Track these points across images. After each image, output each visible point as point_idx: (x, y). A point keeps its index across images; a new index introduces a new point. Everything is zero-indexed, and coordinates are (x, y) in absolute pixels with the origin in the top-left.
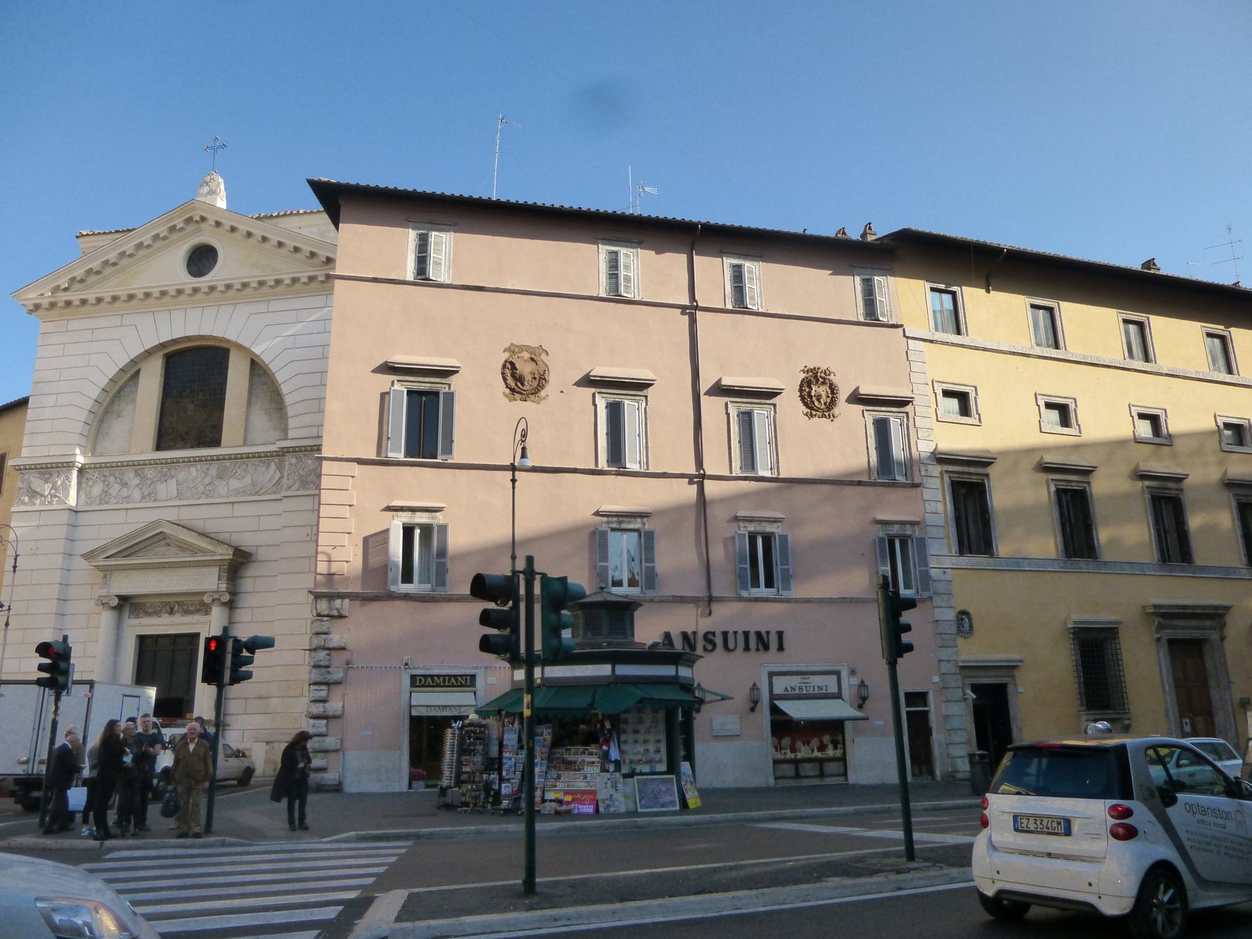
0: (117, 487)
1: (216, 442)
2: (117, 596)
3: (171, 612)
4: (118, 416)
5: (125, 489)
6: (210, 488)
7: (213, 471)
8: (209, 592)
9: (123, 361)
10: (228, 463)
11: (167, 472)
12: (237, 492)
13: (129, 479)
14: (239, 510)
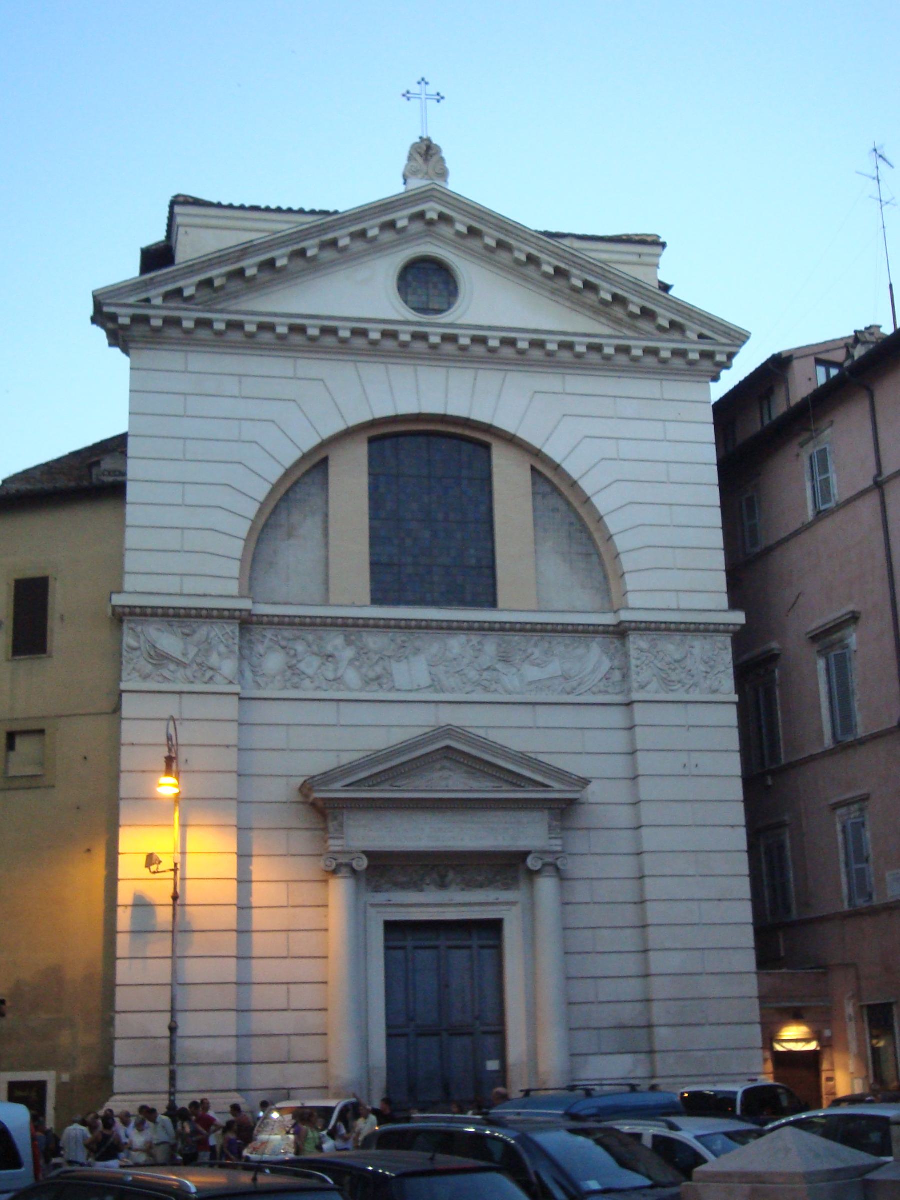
0: (316, 662)
1: (493, 604)
2: (364, 852)
3: (443, 885)
4: (290, 536)
5: (331, 666)
6: (486, 675)
7: (491, 646)
8: (535, 852)
9: (310, 442)
10: (516, 638)
11: (404, 642)
12: (538, 685)
13: (336, 648)
14: (545, 716)
